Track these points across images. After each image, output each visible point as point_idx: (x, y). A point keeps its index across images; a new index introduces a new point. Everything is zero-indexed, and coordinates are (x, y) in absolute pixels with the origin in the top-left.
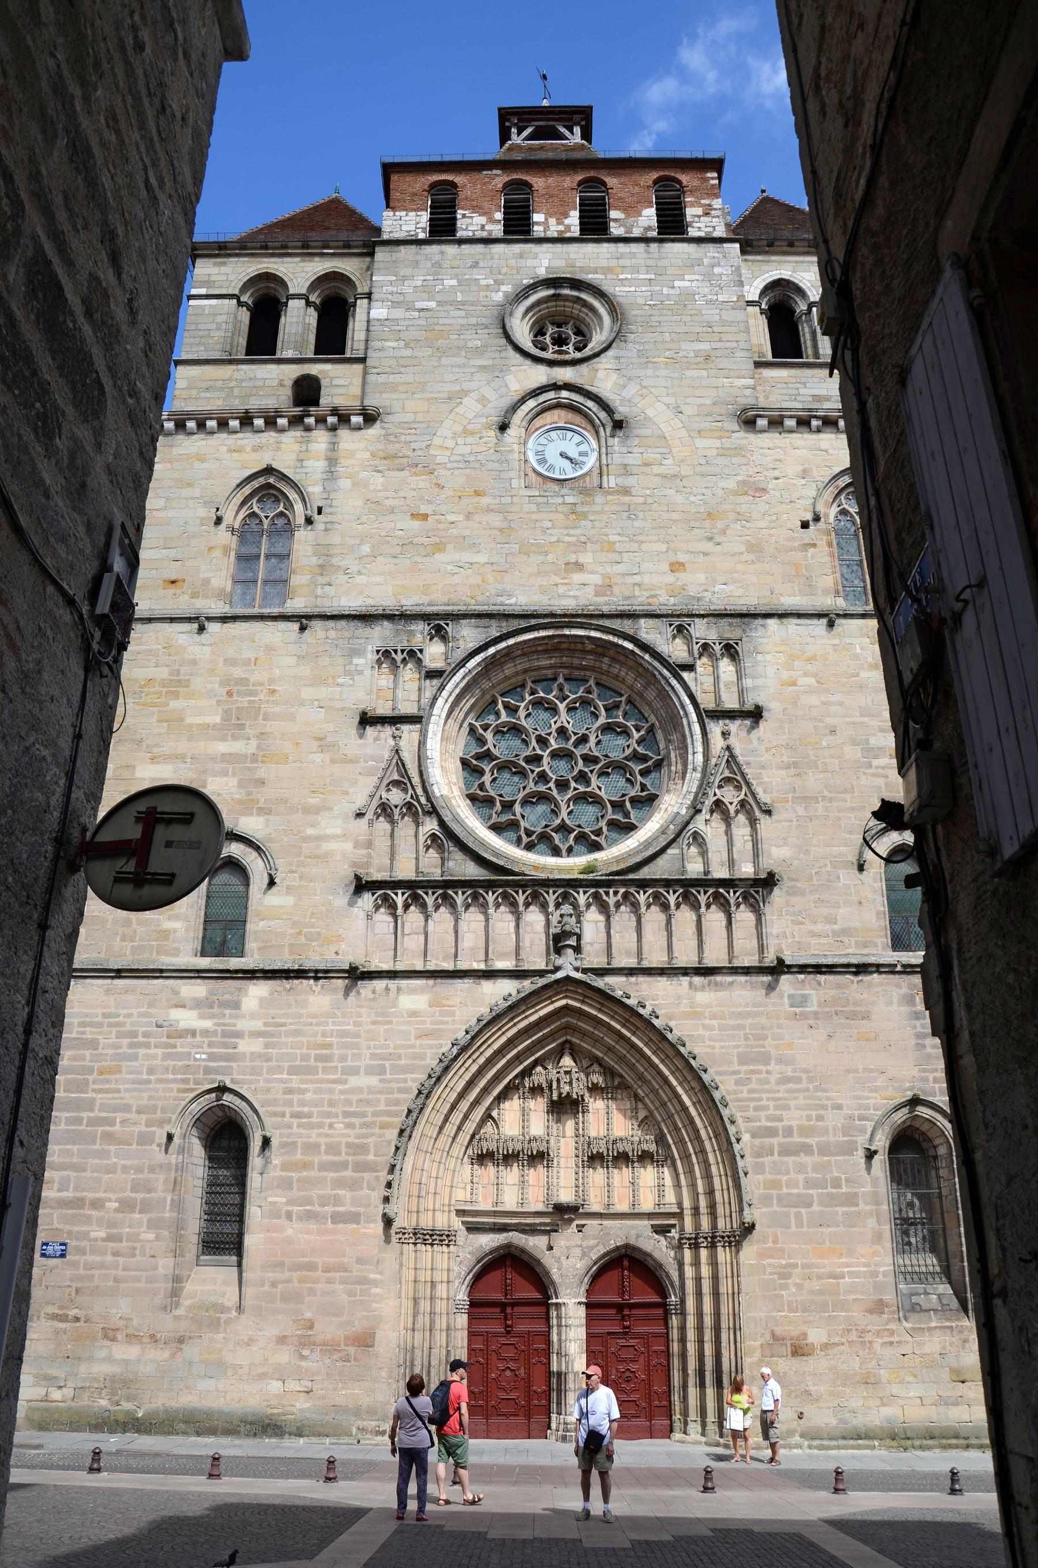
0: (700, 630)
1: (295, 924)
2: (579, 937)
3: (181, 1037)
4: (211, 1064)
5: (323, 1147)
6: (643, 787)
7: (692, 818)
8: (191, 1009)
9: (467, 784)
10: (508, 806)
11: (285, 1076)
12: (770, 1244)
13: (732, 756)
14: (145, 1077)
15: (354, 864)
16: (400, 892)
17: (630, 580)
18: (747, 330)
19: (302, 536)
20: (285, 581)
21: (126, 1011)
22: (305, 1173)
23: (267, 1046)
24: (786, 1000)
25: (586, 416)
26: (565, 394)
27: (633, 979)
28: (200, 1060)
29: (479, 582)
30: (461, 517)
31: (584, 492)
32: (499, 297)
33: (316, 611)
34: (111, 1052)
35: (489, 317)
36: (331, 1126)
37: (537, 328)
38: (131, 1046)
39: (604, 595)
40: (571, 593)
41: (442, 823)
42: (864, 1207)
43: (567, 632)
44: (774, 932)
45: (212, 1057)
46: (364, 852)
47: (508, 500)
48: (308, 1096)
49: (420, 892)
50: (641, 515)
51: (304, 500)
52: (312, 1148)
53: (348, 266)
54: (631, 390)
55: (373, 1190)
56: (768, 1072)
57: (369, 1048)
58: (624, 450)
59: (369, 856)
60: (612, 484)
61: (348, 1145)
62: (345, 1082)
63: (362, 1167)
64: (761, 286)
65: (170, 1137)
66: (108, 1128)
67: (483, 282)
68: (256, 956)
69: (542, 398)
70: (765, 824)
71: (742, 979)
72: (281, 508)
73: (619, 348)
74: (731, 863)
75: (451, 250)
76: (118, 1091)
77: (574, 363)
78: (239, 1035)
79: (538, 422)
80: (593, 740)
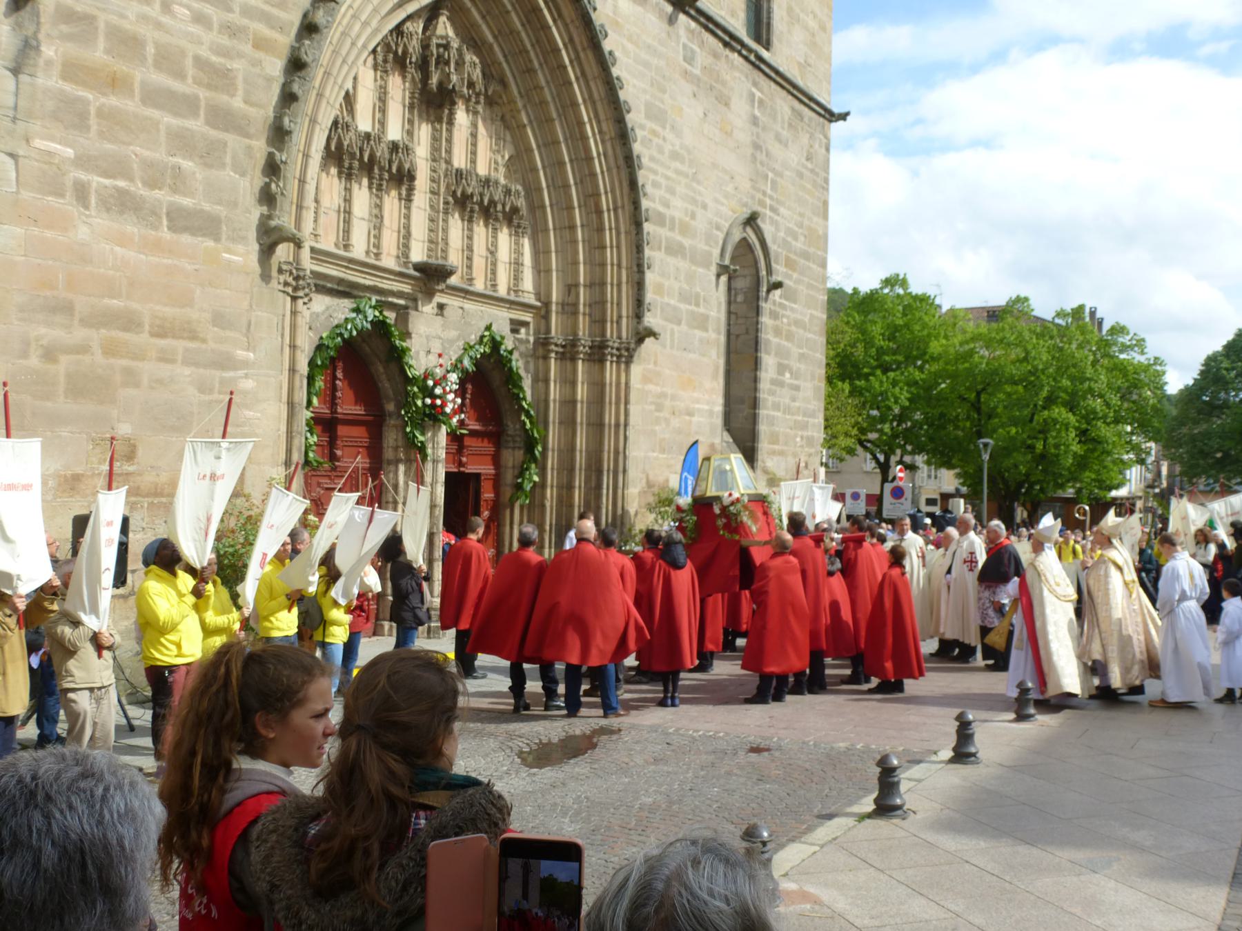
5: (150, 50)
12: (651, 366)
22: (113, 101)
42: (712, 335)
52: (127, 43)
55: (243, 174)
56: (664, 139)
61: (199, 62)
63: (221, 118)
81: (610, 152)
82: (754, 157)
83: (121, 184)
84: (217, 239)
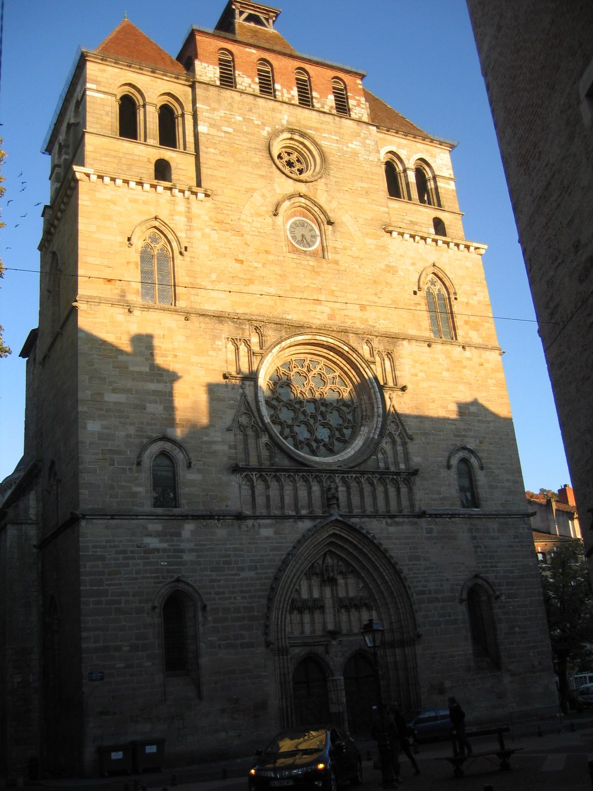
2: (338, 499)
3: (151, 553)
4: (170, 568)
5: (232, 609)
8: (155, 537)
11: (209, 573)
14: (135, 576)
15: (230, 458)
16: (254, 473)
21: (119, 539)
23: (198, 557)
24: (424, 530)
26: (302, 200)
27: (363, 520)
28: (164, 565)
29: (274, 306)
30: (260, 266)
34: (113, 562)
35: (262, 145)
36: (235, 598)
38: (125, 558)
40: (317, 316)
43: (318, 337)
45: (170, 564)
46: (234, 451)
47: (282, 259)
48: (222, 583)
49: (263, 473)
50: (345, 278)
54: (334, 205)
56: (420, 565)
57: (248, 557)
58: (334, 238)
62: (239, 575)
65: (154, 608)
66: (118, 606)
67: (256, 122)
68: (186, 507)
69: (293, 200)
71: (406, 520)
73: (326, 178)
76: (121, 584)
78: (182, 551)
81: (394, 578)
82: (476, 552)
83: (229, 642)
84: (254, 648)
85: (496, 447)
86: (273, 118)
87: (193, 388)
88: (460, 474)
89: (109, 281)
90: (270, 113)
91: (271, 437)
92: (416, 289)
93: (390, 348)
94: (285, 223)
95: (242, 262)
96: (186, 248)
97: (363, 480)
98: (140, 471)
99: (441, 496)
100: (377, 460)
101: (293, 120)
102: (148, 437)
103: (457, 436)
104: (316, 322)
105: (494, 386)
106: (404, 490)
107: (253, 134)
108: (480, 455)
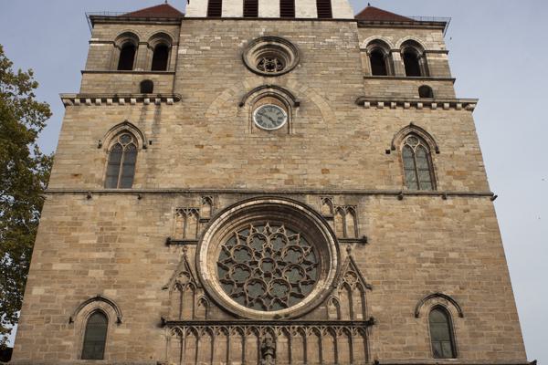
0: (336, 201)
1: (130, 343)
2: (274, 350)
6: (308, 277)
7: (332, 291)
9: (219, 274)
10: (240, 285)
13: (352, 261)
15: (161, 313)
17: (301, 177)
18: (360, 62)
19: (141, 154)
20: (132, 176)
25: (282, 101)
26: (271, 90)
30: (220, 147)
31: (280, 135)
32: (241, 45)
33: (147, 190)
37: (259, 60)
39: (289, 184)
41: (206, 293)
43: (270, 201)
44: (374, 348)
46: (166, 307)
47: (242, 139)
49: (194, 327)
51: (143, 138)
53: (169, 29)
54: (304, 89)
59: (169, 309)
60: (294, 132)
64: (367, 42)
69: (261, 92)
70: (369, 295)
72: (132, 141)
74: (351, 314)
75: (218, 23)
77: (276, 76)
79: (259, 103)
80: (283, 254)
85: (482, 292)
86: (251, 33)
87: (135, 254)
88: (432, 323)
89: (76, 175)
90: (248, 29)
91: (206, 293)
92: (389, 148)
93: (351, 203)
94: (251, 111)
95: (202, 146)
96: (150, 143)
97: (306, 331)
98: (72, 328)
99: (405, 346)
100: (327, 311)
101: (270, 30)
102: (84, 298)
103: (430, 283)
104: (272, 188)
105: (482, 230)
106: (358, 340)
107: (228, 48)
108: (460, 301)
